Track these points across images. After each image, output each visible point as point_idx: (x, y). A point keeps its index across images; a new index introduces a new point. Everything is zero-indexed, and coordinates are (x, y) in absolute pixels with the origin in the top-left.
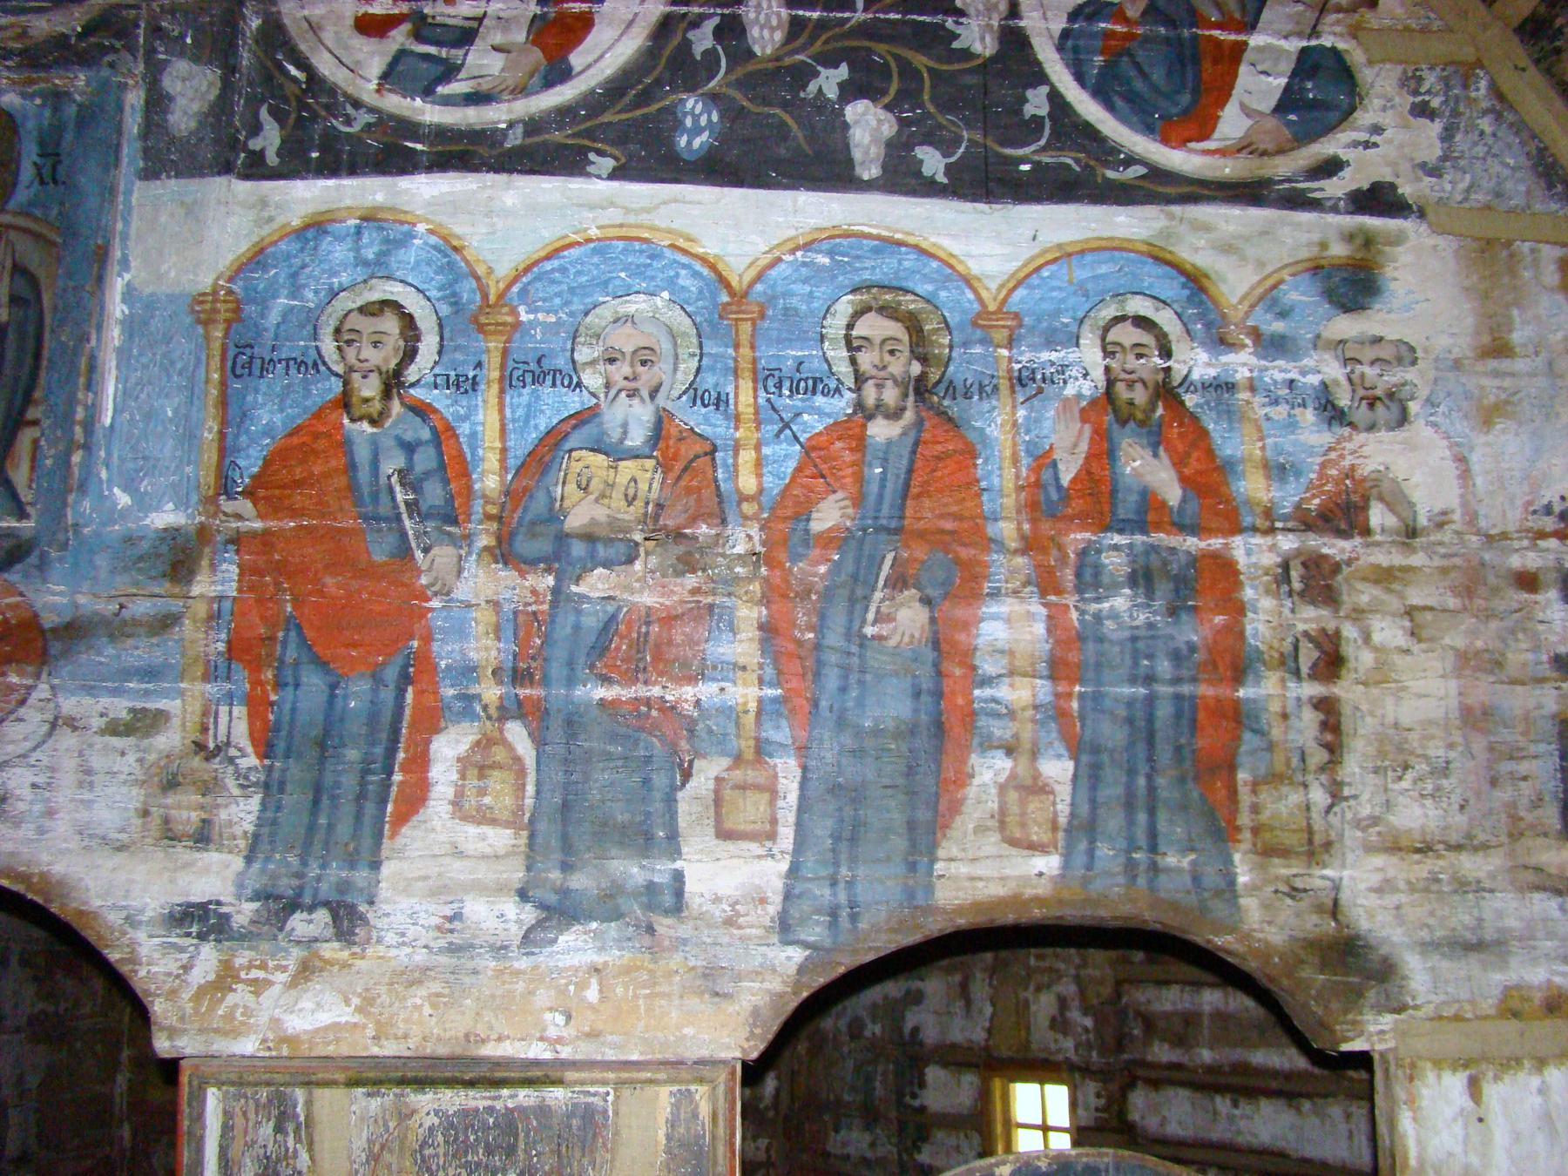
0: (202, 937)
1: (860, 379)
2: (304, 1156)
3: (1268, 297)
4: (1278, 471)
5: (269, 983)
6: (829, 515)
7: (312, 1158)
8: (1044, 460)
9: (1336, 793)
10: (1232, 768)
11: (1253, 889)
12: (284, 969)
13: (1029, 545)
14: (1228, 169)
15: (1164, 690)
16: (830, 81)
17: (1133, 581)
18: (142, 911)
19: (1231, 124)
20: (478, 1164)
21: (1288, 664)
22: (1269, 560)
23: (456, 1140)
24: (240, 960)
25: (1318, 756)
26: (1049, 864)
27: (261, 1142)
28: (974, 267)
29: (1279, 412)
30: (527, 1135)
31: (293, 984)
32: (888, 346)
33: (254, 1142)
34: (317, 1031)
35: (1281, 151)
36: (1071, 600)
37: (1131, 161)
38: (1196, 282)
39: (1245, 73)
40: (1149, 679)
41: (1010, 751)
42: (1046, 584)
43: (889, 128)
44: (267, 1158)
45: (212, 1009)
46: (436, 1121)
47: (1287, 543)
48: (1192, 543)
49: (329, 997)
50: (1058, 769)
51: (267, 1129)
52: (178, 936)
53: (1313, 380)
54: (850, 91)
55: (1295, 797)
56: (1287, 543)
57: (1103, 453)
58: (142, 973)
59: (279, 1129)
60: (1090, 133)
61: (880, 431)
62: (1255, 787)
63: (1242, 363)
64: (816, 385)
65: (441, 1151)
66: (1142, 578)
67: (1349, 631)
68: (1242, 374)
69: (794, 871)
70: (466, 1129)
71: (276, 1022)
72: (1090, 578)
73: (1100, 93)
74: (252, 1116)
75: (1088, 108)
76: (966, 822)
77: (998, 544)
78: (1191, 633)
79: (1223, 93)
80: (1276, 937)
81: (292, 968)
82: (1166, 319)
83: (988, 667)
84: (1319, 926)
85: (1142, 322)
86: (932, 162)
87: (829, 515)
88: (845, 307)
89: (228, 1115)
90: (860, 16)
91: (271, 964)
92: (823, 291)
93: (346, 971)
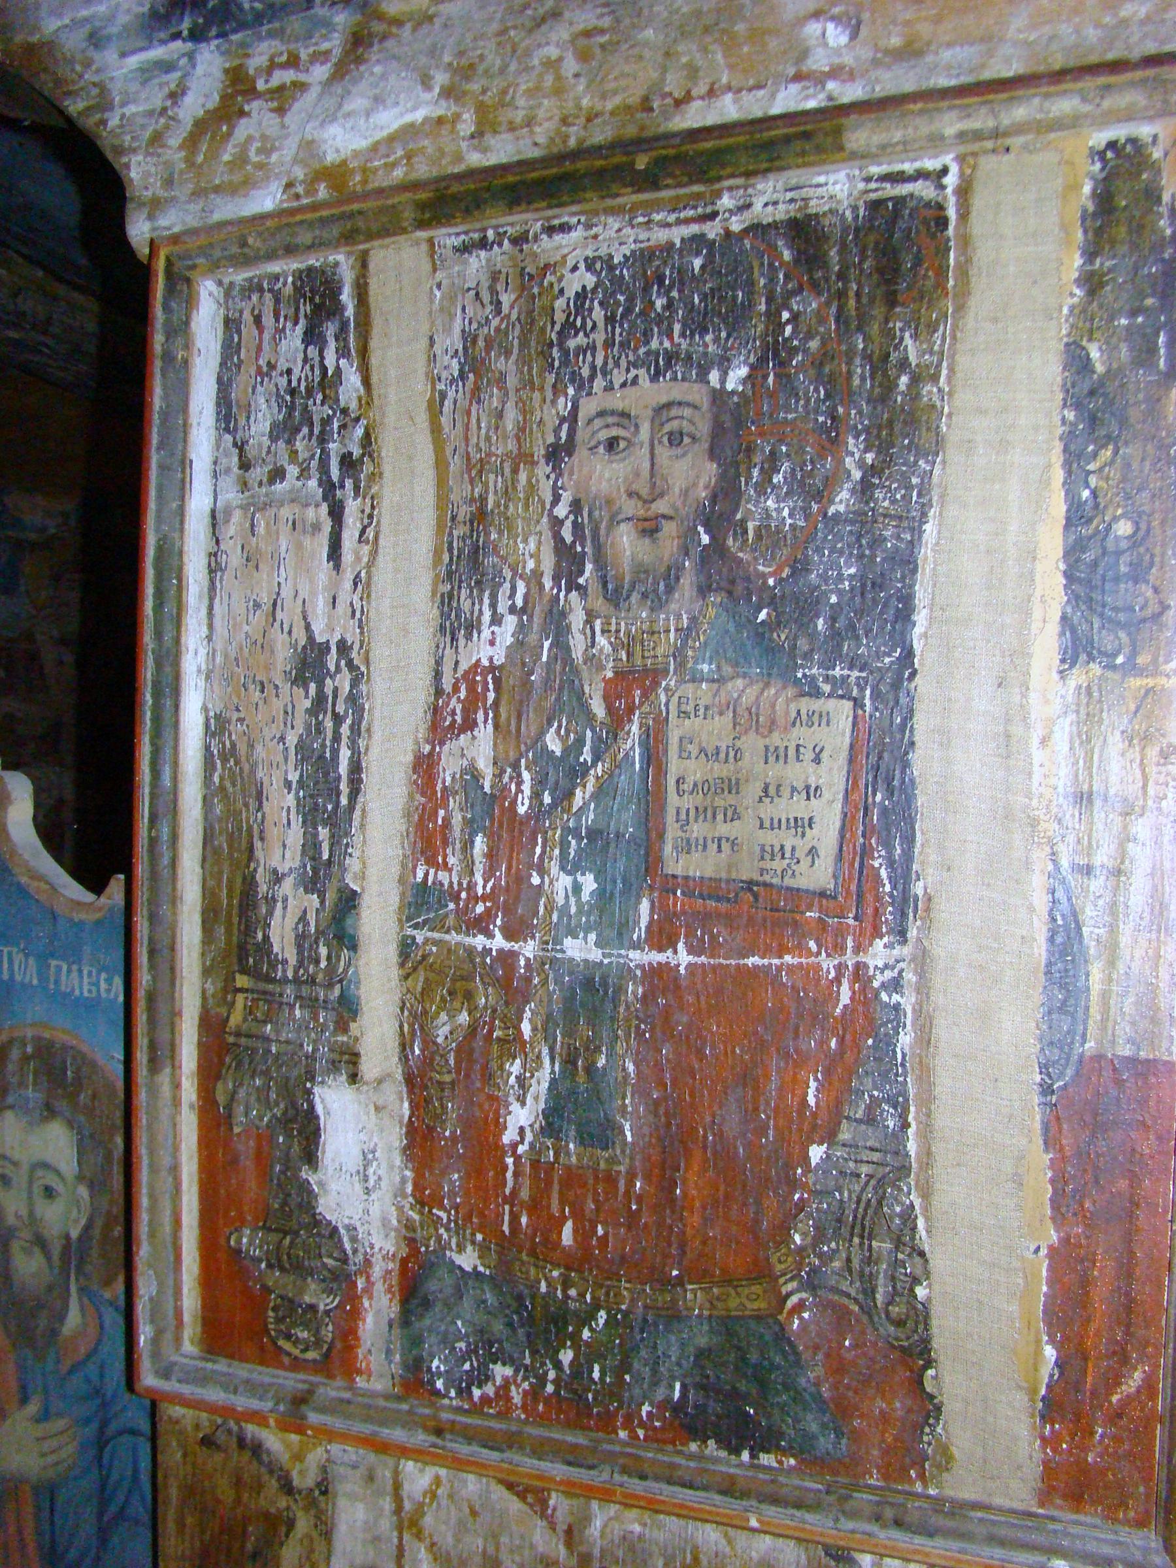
0: (197, 36)
2: (352, 379)
5: (301, 87)
7: (366, 382)
12: (320, 57)
18: (111, 18)
20: (671, 357)
23: (628, 311)
24: (257, 61)
27: (282, 365)
30: (772, 280)
31: (340, 73)
33: (271, 366)
34: (375, 148)
44: (293, 392)
45: (213, 155)
46: (590, 280)
49: (399, 80)
51: (294, 339)
52: (163, 42)
58: (114, 122)
59: (312, 336)
65: (599, 337)
70: (646, 289)
71: (309, 146)
74: (268, 320)
81: (335, 43)
89: (231, 324)
91: (304, 55)
93: (425, 29)
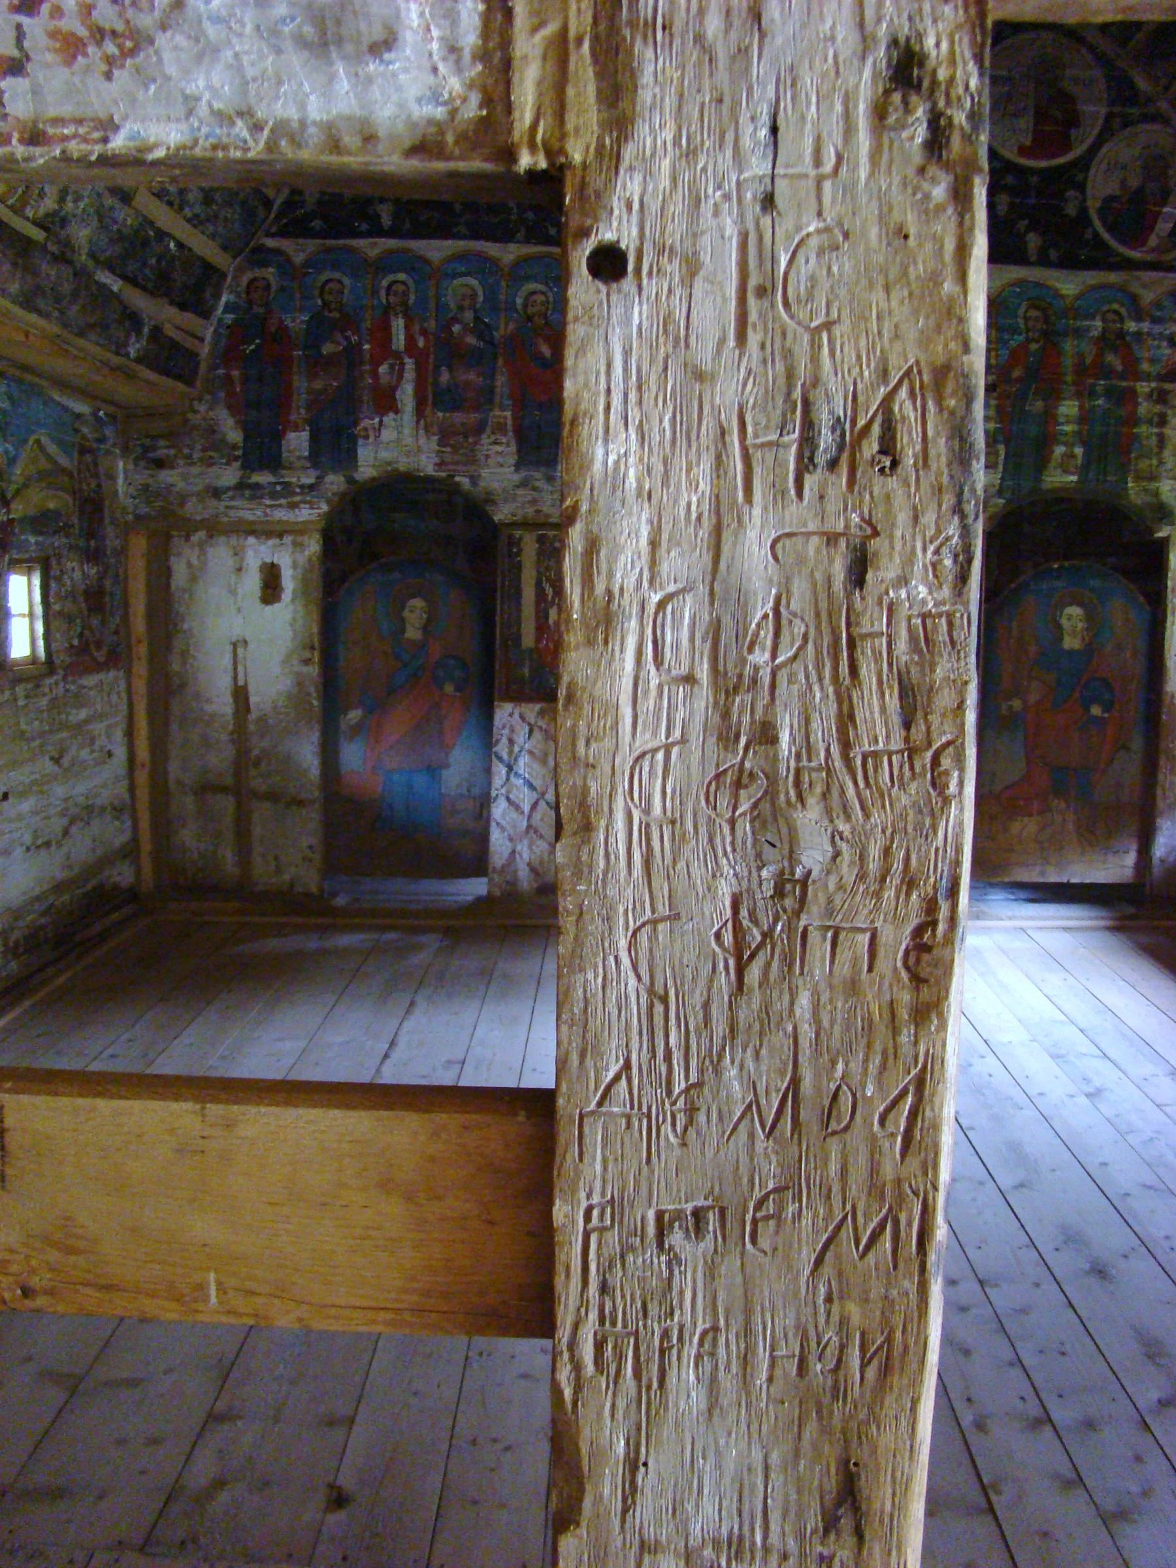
1: (1028, 330)
3: (1157, 304)
4: (1152, 361)
6: (1017, 373)
8: (1081, 356)
9: (1161, 463)
10: (1129, 452)
11: (1132, 488)
13: (1075, 384)
14: (1149, 258)
15: (1112, 429)
16: (1022, 225)
17: (1105, 395)
19: (1153, 241)
21: (1150, 422)
22: (1147, 390)
25: (1155, 450)
26: (1074, 478)
28: (1064, 292)
29: (1156, 342)
32: (1037, 319)
35: (1168, 251)
36: (1086, 400)
37: (1118, 254)
38: (1134, 299)
39: (1160, 220)
40: (1108, 425)
41: (1065, 444)
42: (1078, 395)
43: (1039, 243)
47: (1153, 385)
48: (1124, 384)
50: (1079, 451)
53: (1168, 332)
54: (1029, 229)
55: (1147, 462)
56: (1153, 385)
57: (1100, 355)
60: (1103, 244)
61: (1034, 347)
62: (1137, 458)
63: (1145, 326)
64: (1015, 331)
66: (1109, 393)
67: (1169, 412)
68: (1146, 330)
69: (1002, 479)
72: (1092, 394)
73: (1110, 229)
75: (1106, 236)
76: (1053, 464)
77: (1066, 383)
78: (1122, 412)
79: (1152, 228)
80: (1139, 502)
82: (1123, 311)
83: (1061, 420)
84: (1149, 499)
85: (1115, 312)
86: (1053, 254)
87: (1017, 373)
88: (1024, 305)
90: (1033, 201)
92: (1017, 301)
